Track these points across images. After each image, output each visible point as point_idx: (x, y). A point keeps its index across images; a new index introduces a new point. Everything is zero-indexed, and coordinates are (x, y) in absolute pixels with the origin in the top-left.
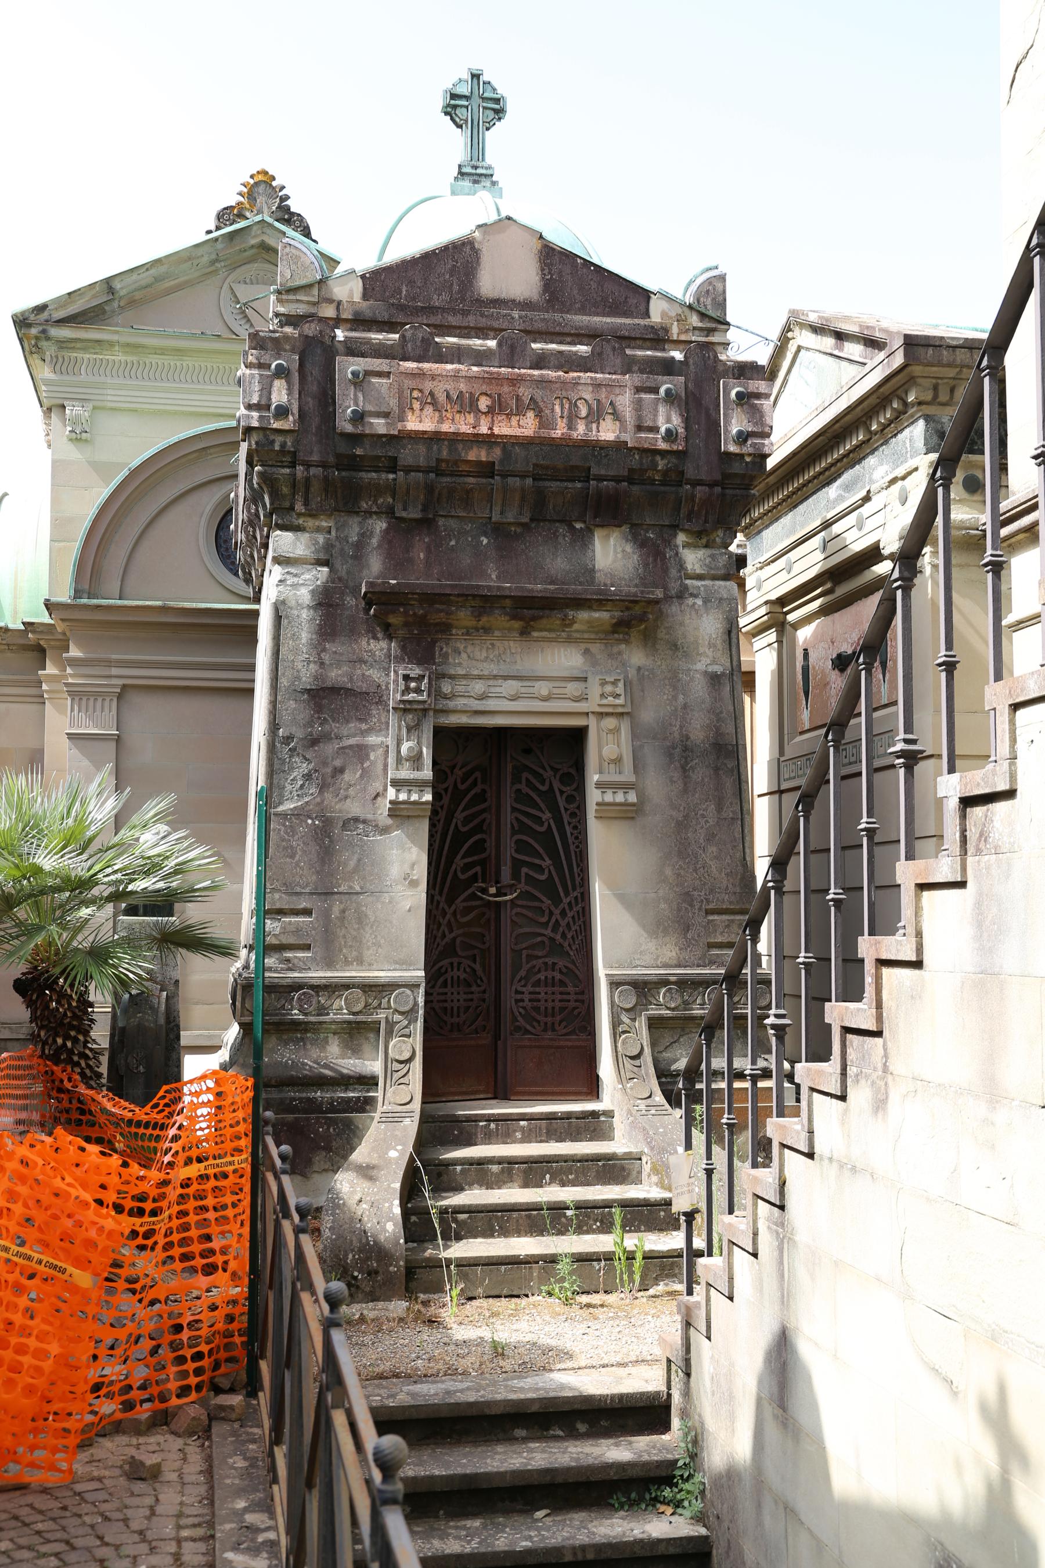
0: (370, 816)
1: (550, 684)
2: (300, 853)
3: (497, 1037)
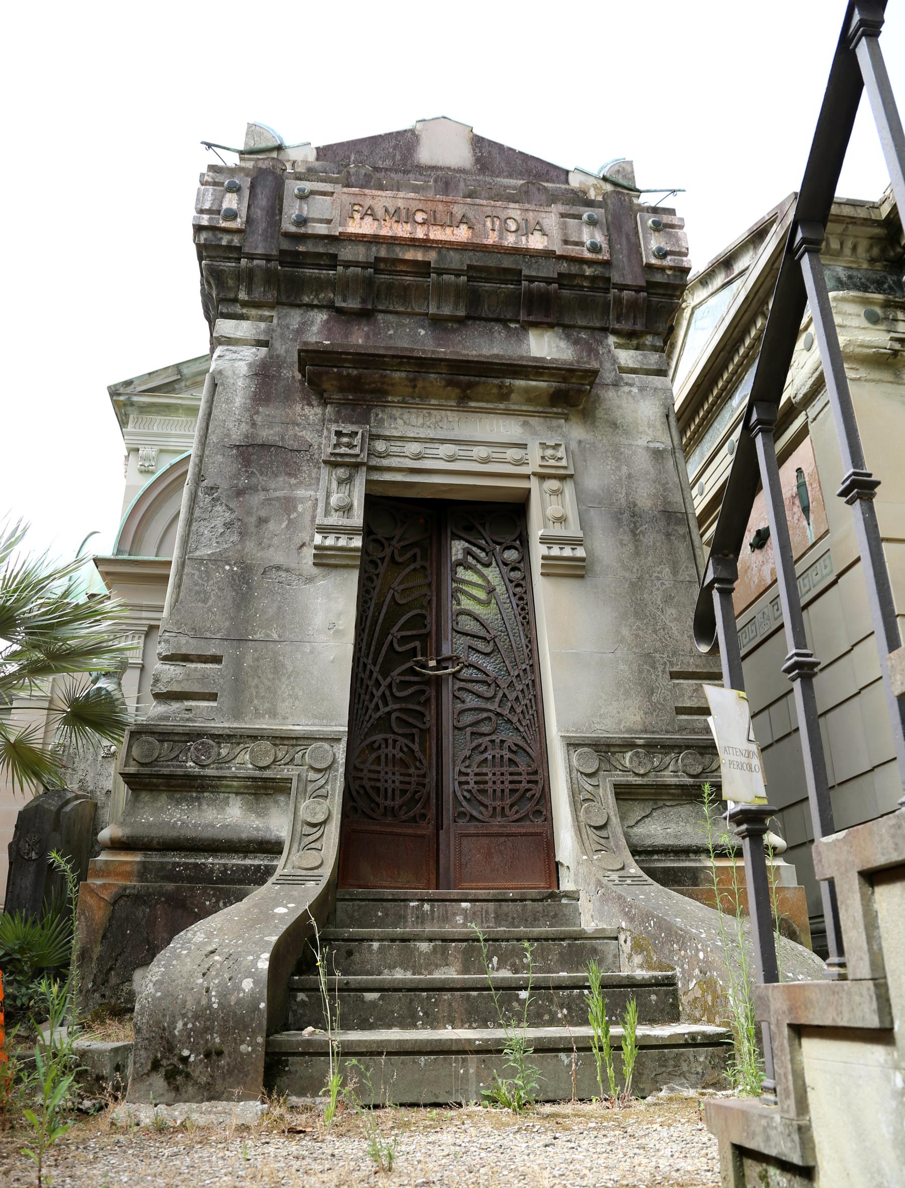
0: (293, 565)
1: (490, 450)
2: (213, 598)
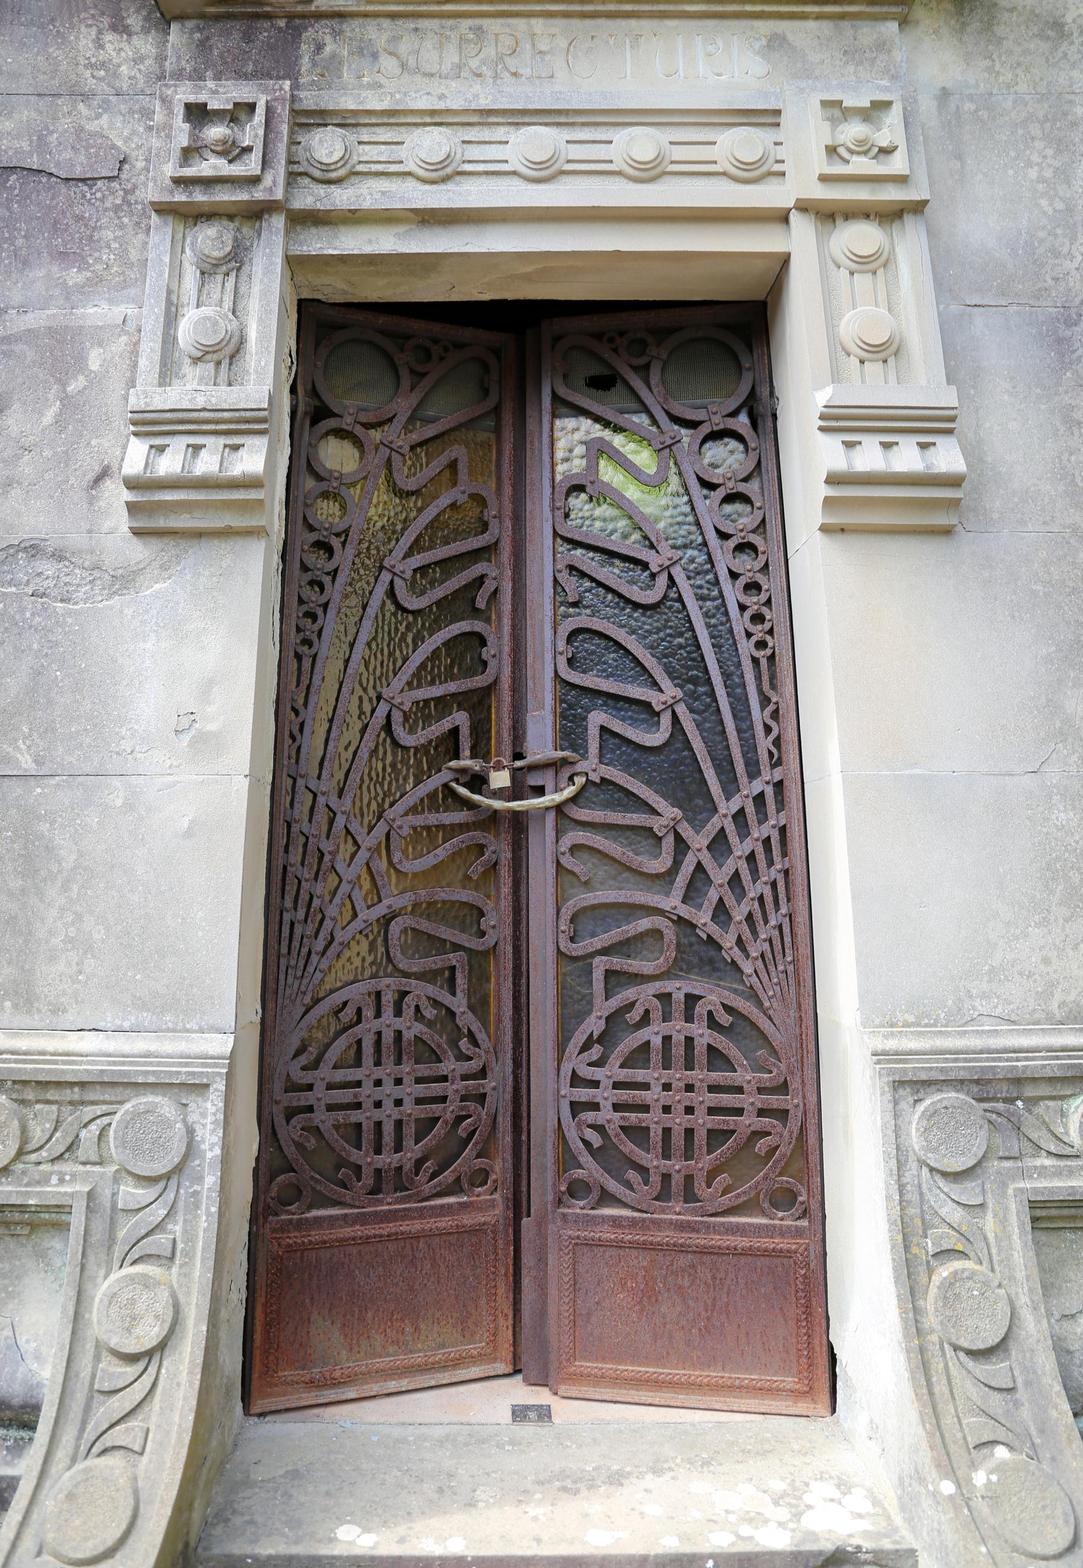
0: (76, 539)
3: (518, 1205)
